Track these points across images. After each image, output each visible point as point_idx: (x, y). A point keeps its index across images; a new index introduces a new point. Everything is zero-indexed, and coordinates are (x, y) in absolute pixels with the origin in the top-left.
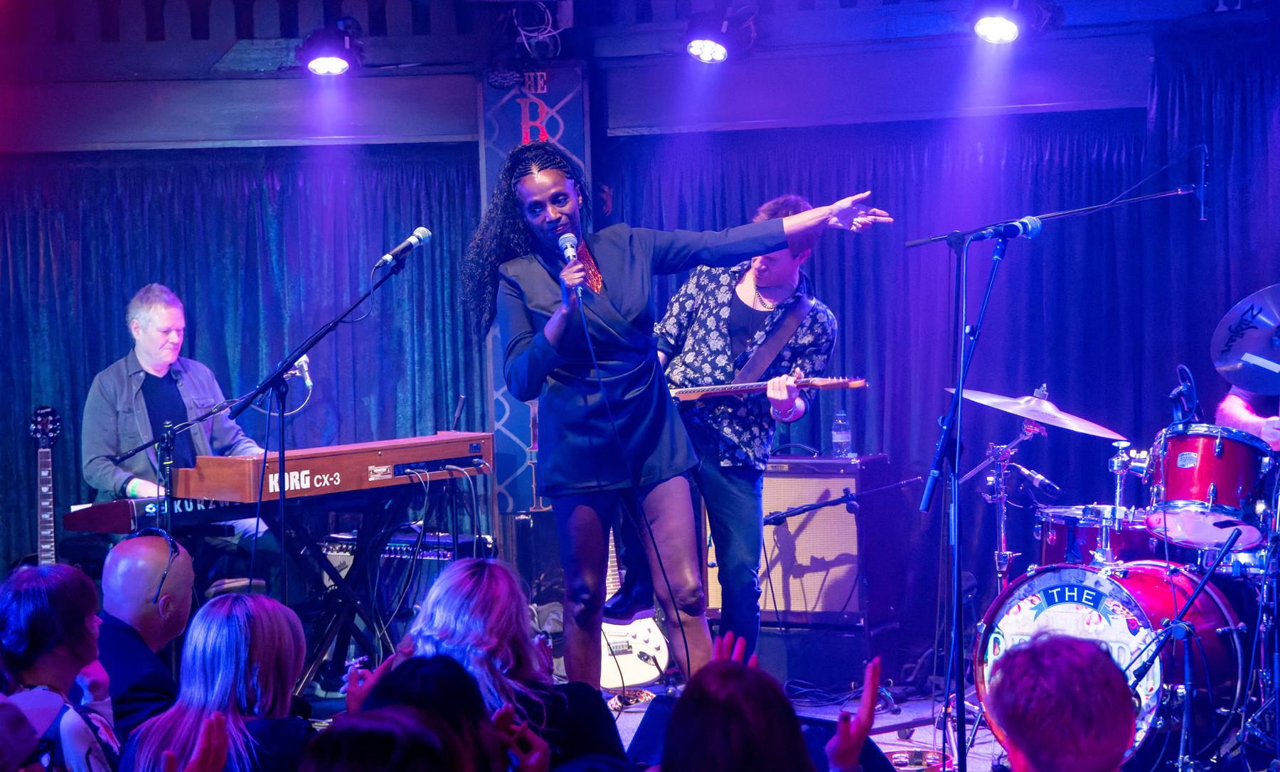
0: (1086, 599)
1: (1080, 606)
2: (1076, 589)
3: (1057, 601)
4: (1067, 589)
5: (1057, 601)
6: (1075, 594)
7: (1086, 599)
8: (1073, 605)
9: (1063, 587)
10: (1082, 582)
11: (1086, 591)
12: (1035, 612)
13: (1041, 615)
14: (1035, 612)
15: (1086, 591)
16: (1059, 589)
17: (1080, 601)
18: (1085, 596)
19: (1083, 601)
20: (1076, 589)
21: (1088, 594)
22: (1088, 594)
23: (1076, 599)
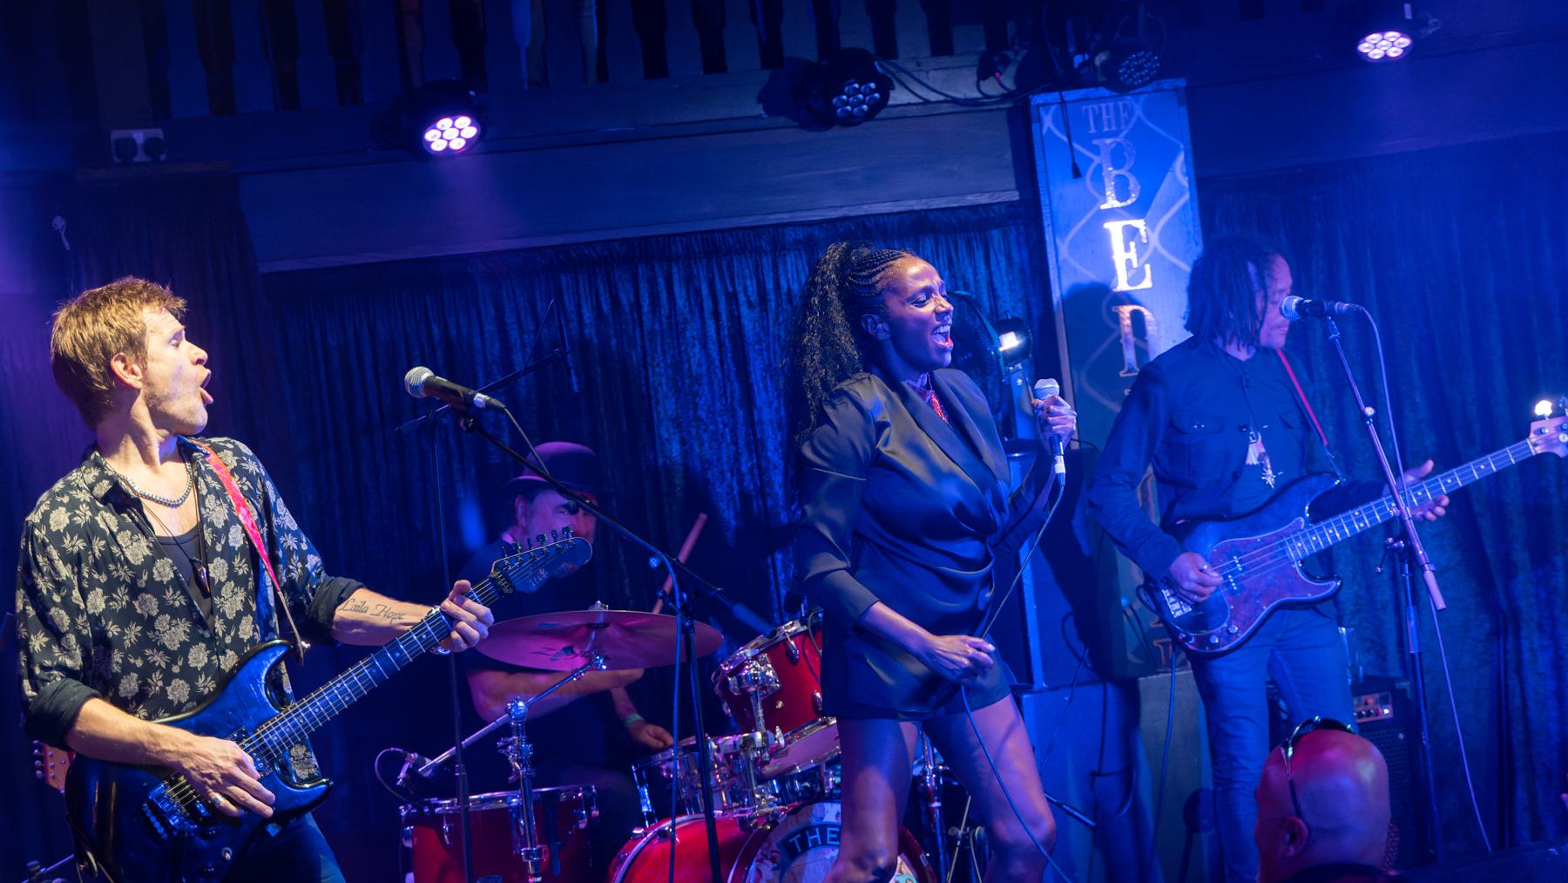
0: (832, 839)
1: (825, 849)
2: (817, 830)
3: (800, 850)
4: (808, 832)
5: (800, 850)
6: (818, 836)
7: (832, 839)
8: (819, 849)
9: (802, 832)
10: (822, 818)
11: (829, 829)
12: (778, 872)
13: (786, 874)
14: (778, 872)
15: (829, 829)
16: (799, 836)
17: (824, 843)
18: (829, 836)
19: (829, 842)
20: (817, 830)
21: (832, 832)
22: (832, 832)
23: (820, 843)
